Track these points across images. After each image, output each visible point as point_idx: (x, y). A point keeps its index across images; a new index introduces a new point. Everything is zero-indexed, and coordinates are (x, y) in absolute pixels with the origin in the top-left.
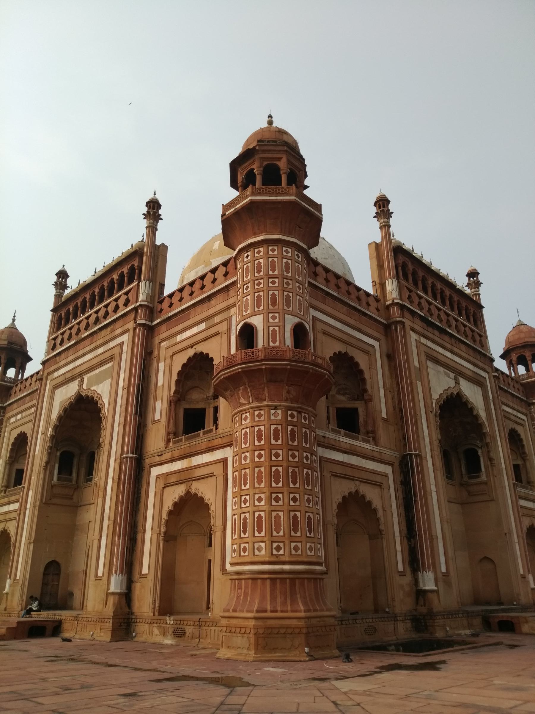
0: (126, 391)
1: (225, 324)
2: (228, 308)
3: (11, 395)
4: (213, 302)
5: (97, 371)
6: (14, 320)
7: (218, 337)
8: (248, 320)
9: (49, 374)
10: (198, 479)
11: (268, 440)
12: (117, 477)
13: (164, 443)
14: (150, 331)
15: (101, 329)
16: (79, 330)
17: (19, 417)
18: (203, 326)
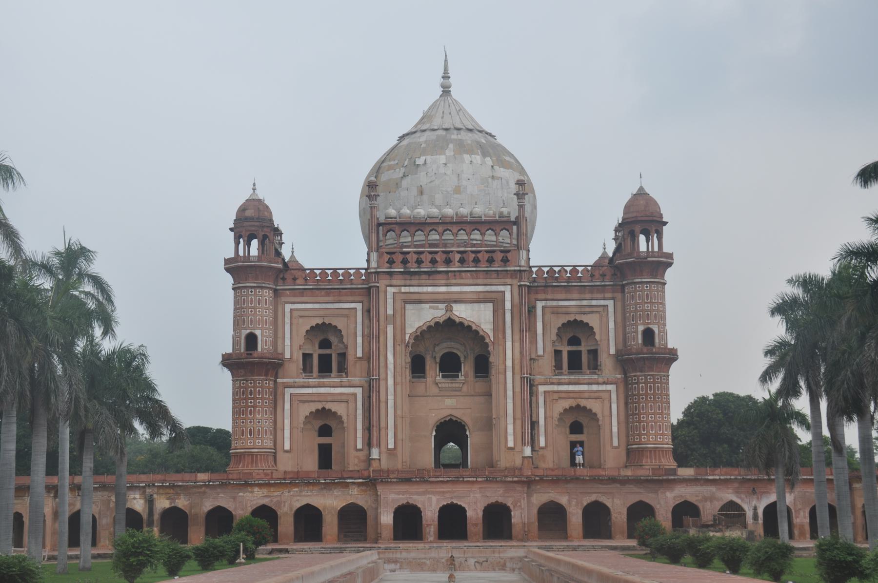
3: (284, 279)
7: (598, 315)
8: (650, 326)
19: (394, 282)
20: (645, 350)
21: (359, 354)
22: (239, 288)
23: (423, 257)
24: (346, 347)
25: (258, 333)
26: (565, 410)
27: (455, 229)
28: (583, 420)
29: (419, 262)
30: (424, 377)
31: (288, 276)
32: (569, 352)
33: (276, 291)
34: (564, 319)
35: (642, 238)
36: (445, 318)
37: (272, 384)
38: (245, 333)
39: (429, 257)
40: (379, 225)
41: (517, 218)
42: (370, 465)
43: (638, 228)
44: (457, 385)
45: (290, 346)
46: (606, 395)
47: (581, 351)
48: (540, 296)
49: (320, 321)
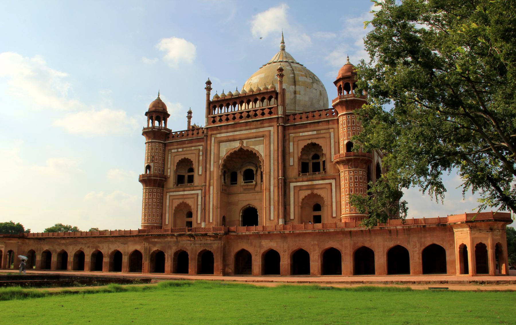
0: (276, 152)
1: (328, 135)
2: (329, 129)
3: (169, 137)
4: (320, 124)
5: (253, 140)
6: (159, 95)
9: (211, 135)
10: (317, 189)
11: (359, 180)
12: (276, 185)
13: (298, 174)
14: (284, 128)
15: (253, 121)
16: (234, 118)
17: (180, 150)
18: (315, 132)
21: (200, 173)
25: (152, 165)
26: (306, 197)
30: (236, 184)
31: (171, 136)
32: (313, 163)
33: (165, 145)
34: (306, 143)
36: (239, 148)
38: (146, 165)
45: (171, 172)
46: (329, 185)
47: (319, 163)
48: (292, 131)
49: (183, 157)
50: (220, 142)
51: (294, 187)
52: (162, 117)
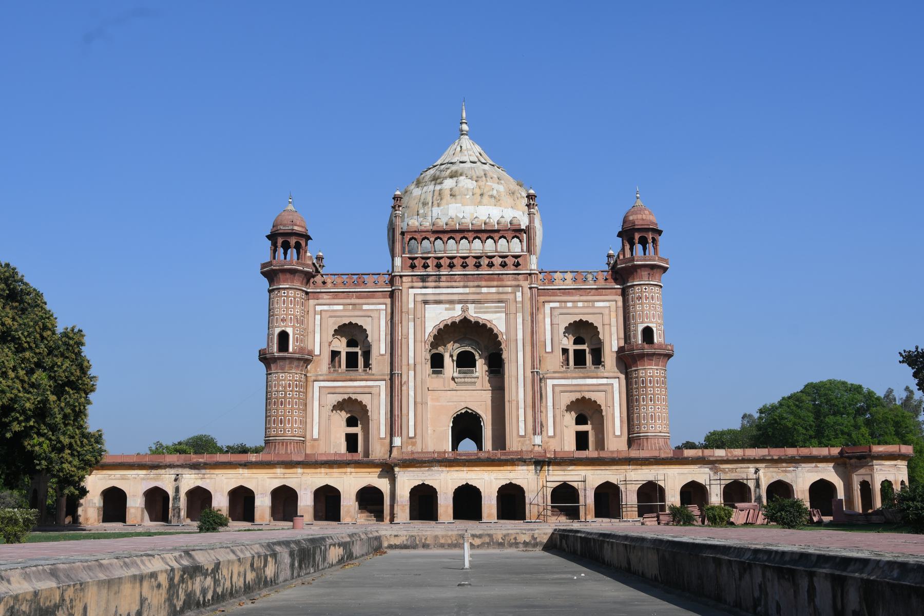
8: (650, 325)
19: (415, 284)
20: (646, 346)
21: (383, 351)
22: (273, 290)
23: (442, 261)
24: (369, 346)
25: (290, 331)
26: (572, 402)
27: (471, 236)
28: (587, 413)
29: (439, 266)
31: (318, 279)
32: (575, 350)
35: (639, 248)
37: (303, 379)
39: (448, 261)
40: (403, 233)
41: (528, 227)
42: (391, 452)
43: (637, 236)
44: (473, 380)
50: (426, 302)
51: (554, 386)
52: (303, 243)
